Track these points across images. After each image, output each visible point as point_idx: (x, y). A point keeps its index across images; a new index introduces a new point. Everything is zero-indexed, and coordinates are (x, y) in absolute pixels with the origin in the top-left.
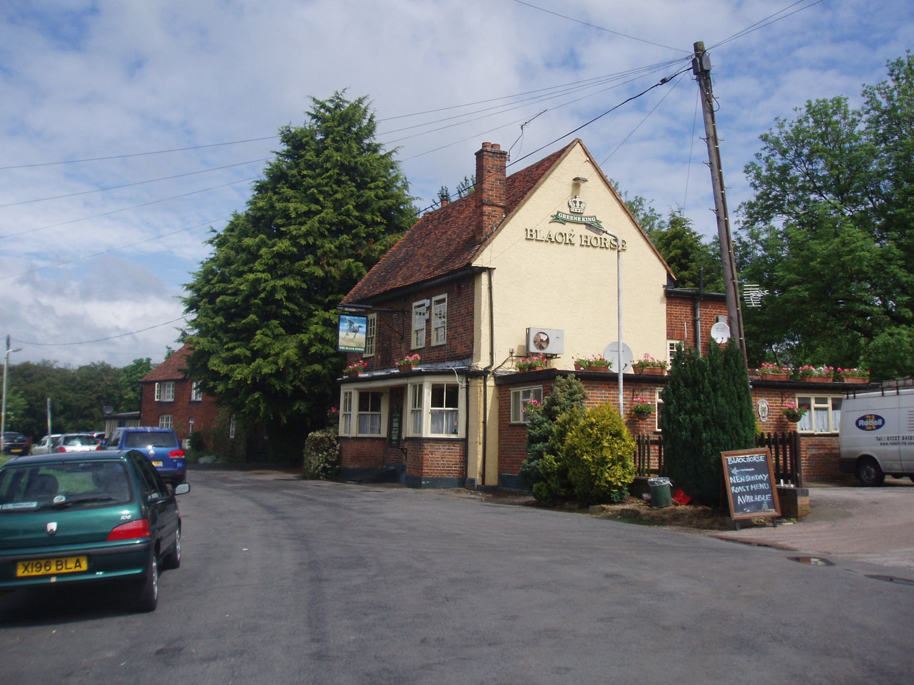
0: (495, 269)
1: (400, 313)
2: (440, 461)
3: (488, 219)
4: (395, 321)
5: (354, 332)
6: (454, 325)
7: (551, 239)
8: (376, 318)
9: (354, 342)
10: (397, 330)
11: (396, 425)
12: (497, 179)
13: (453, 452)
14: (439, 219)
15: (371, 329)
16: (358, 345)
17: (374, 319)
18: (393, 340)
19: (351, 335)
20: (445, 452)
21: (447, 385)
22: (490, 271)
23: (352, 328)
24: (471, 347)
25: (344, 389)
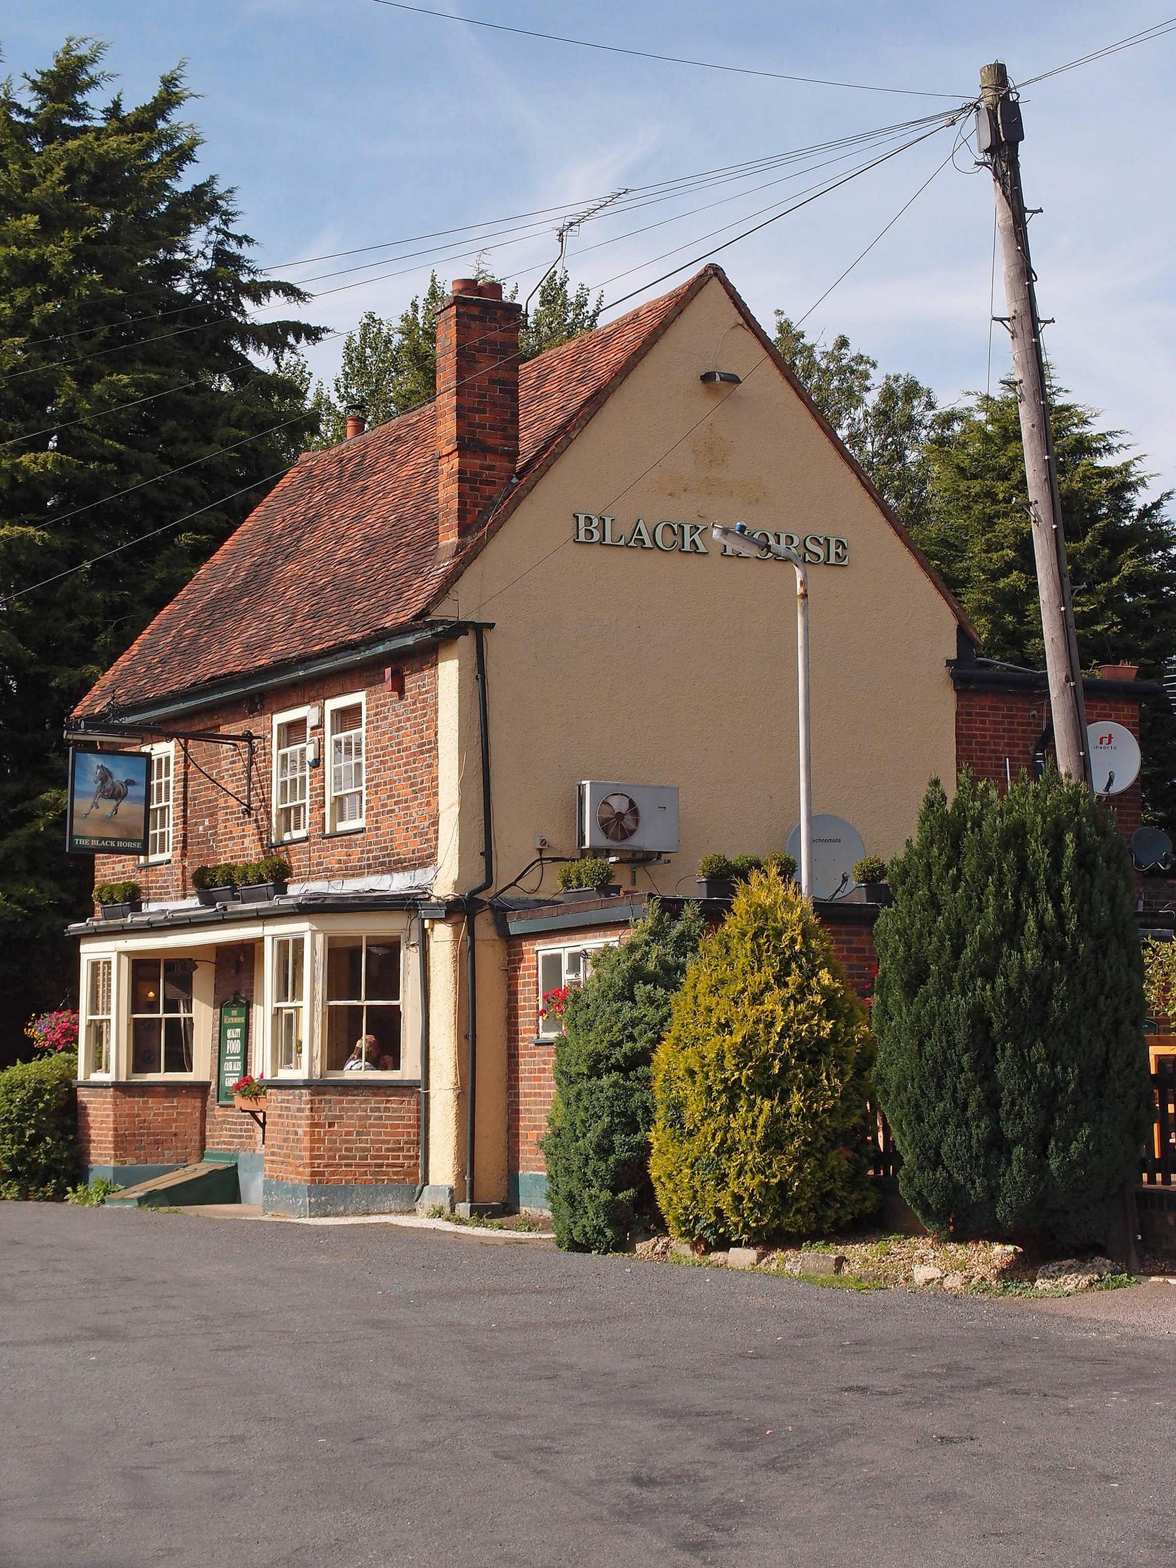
0: (491, 626)
1: (241, 744)
2: (355, 1142)
3: (472, 489)
4: (225, 764)
5: (112, 797)
6: (389, 775)
7: (643, 540)
8: (172, 755)
9: (115, 825)
10: (231, 788)
11: (234, 1046)
12: (493, 381)
13: (388, 1118)
14: (340, 477)
15: (159, 785)
16: (125, 835)
17: (168, 758)
18: (221, 815)
19: (107, 806)
20: (369, 1118)
21: (367, 938)
22: (479, 630)
23: (108, 786)
24: (431, 836)
25: (90, 951)
